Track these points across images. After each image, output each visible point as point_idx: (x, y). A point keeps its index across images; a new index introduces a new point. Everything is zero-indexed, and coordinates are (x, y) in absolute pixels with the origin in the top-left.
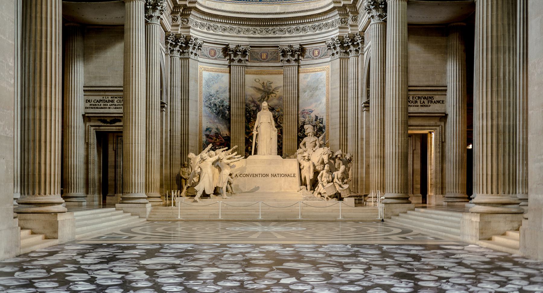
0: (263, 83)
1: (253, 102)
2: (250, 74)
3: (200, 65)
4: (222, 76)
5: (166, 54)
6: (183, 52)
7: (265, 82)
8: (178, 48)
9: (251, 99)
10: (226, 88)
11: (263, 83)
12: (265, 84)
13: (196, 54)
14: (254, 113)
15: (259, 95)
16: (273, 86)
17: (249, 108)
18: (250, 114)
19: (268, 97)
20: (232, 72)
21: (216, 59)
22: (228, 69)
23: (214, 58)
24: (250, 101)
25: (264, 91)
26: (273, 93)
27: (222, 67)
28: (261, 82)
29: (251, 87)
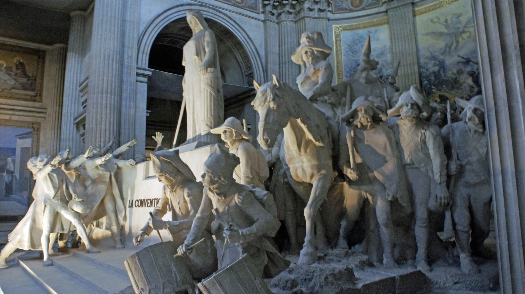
0: (446, 21)
1: (433, 58)
2: (422, 13)
3: (335, 27)
4: (376, 31)
5: (264, 21)
6: (299, 12)
7: (449, 18)
8: (287, 8)
9: (428, 54)
10: (385, 47)
11: (446, 21)
12: (449, 21)
13: (320, 10)
14: (435, 77)
15: (441, 44)
16: (463, 19)
17: (427, 70)
18: (429, 81)
19: (458, 42)
20: (391, 20)
21: (363, 9)
22: (386, 17)
23: (361, 7)
24: (427, 58)
25: (448, 34)
26: (464, 32)
27: (374, 18)
28: (442, 20)
29: (427, 34)
